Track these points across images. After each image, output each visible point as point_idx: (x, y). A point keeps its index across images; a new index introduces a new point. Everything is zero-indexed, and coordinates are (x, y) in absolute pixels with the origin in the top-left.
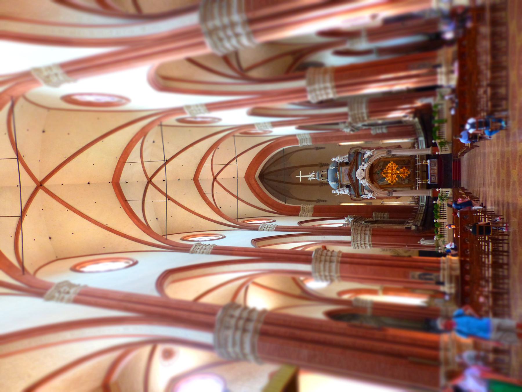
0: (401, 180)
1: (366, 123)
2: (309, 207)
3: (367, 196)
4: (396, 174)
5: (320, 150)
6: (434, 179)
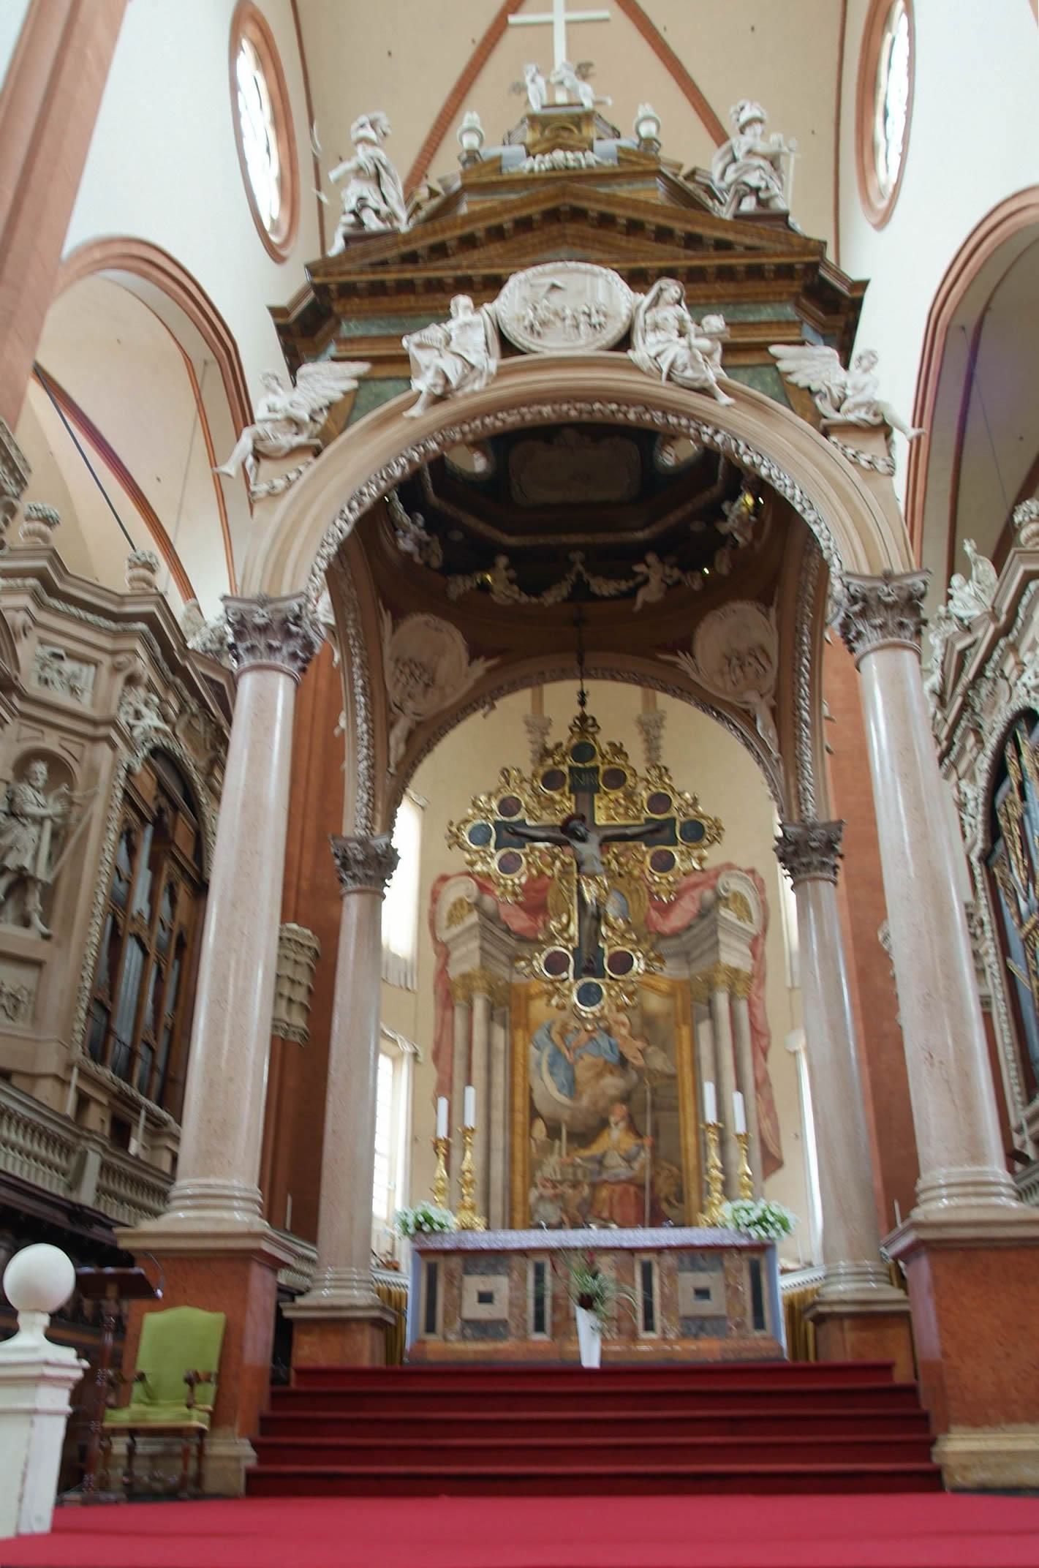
0: (559, 1177)
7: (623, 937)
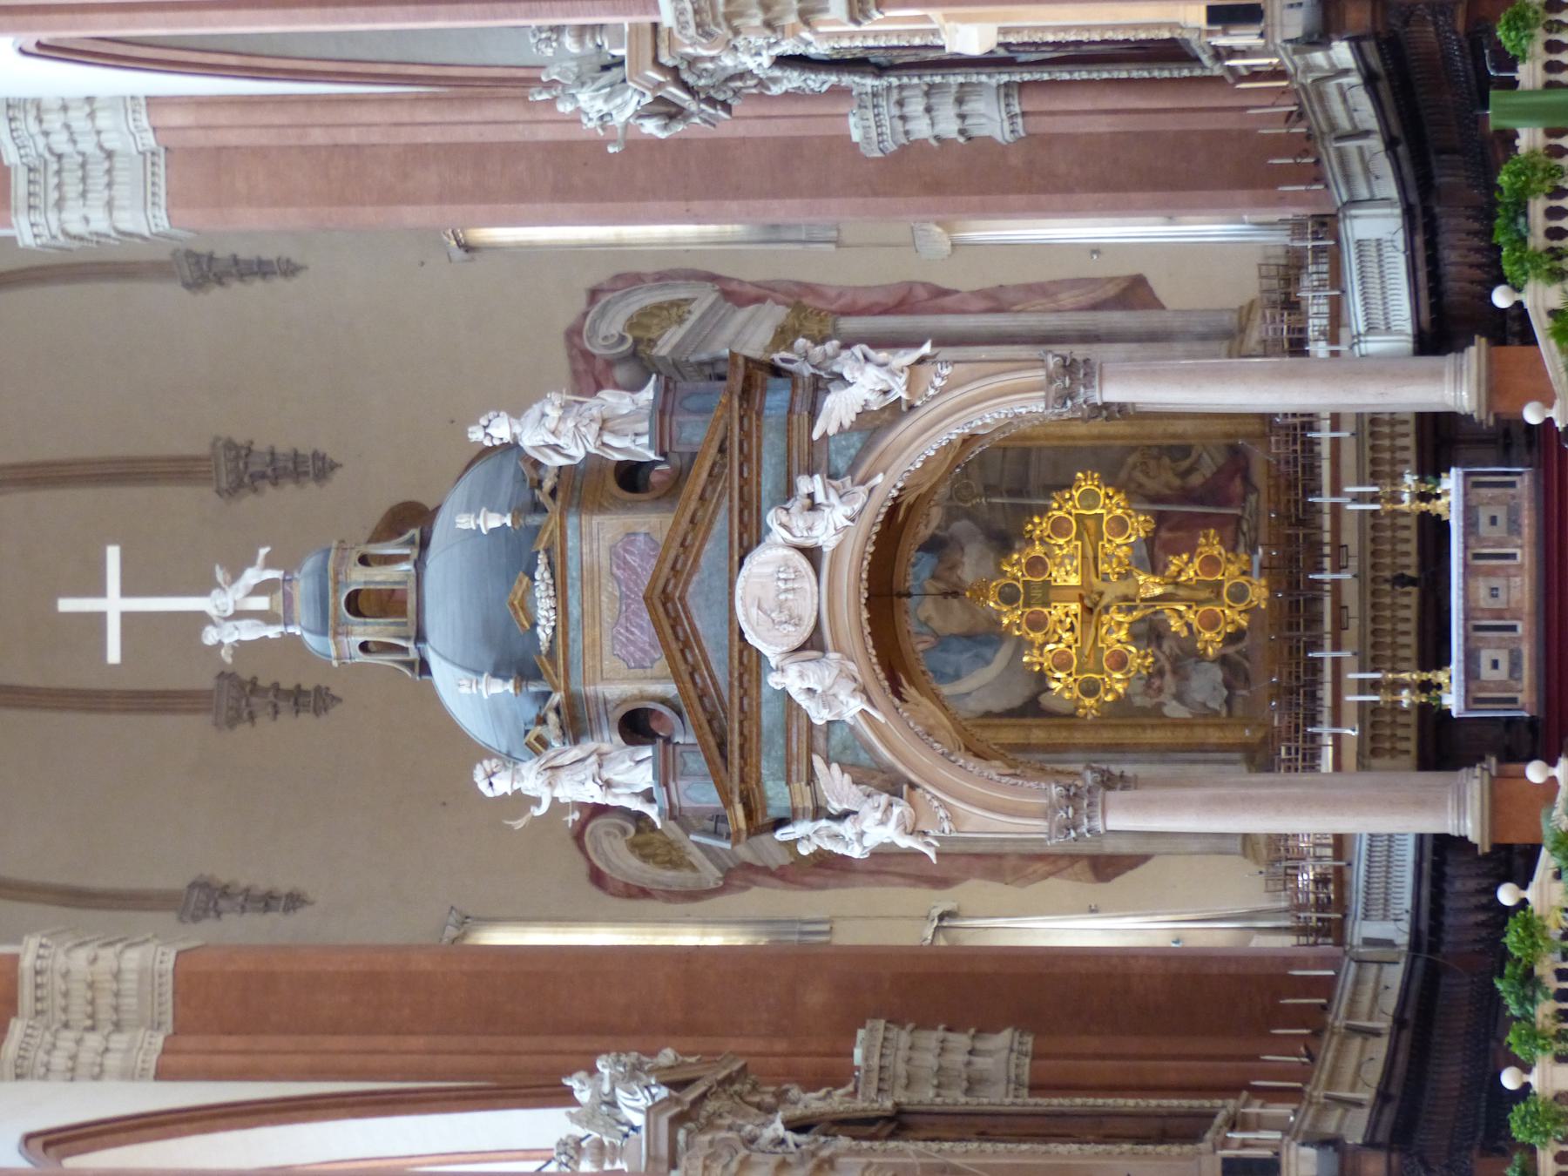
1: (819, 49)
2: (117, 975)
3: (847, 828)
4: (1128, 602)
5: (236, 286)
6: (1504, 665)
7: (1187, 564)
